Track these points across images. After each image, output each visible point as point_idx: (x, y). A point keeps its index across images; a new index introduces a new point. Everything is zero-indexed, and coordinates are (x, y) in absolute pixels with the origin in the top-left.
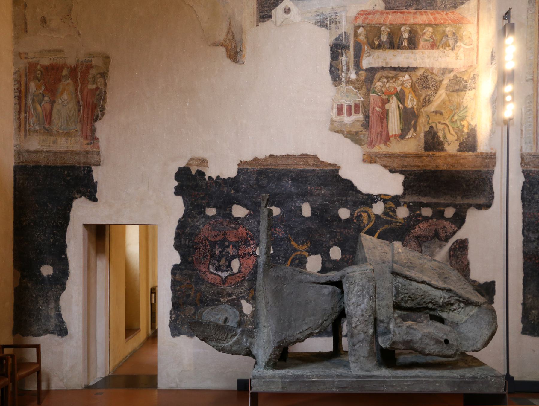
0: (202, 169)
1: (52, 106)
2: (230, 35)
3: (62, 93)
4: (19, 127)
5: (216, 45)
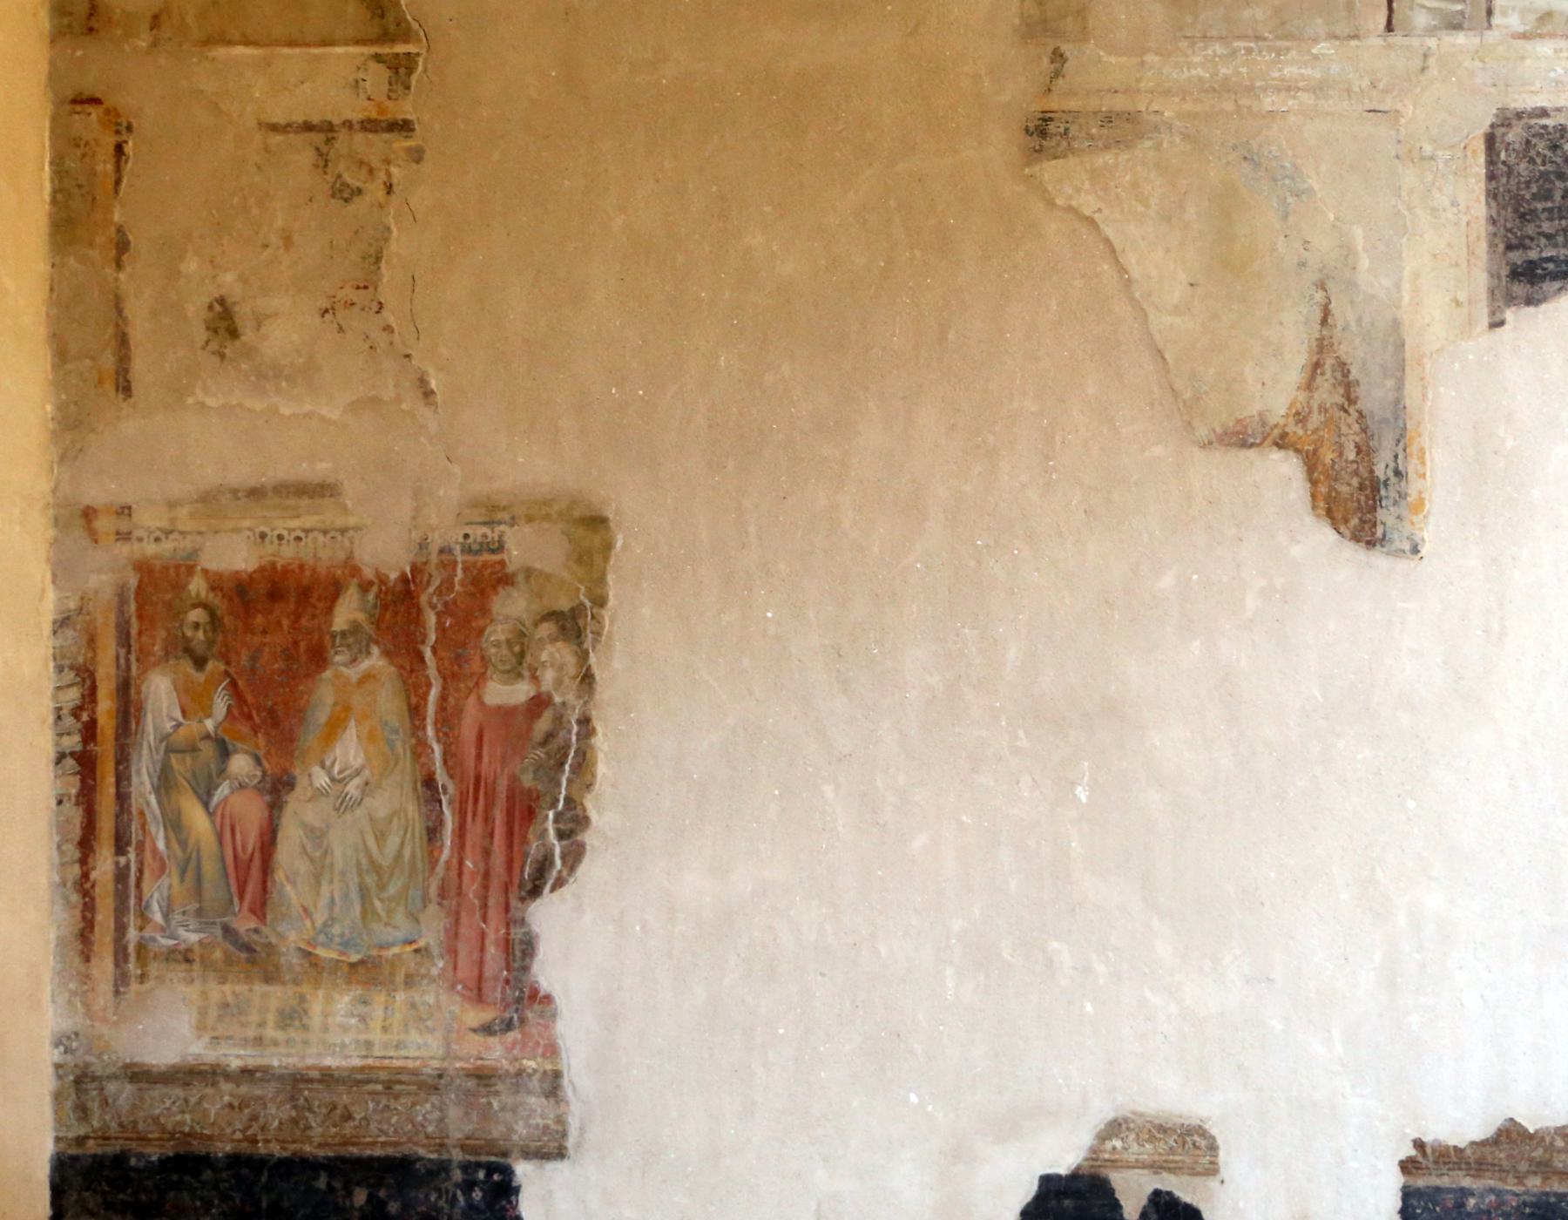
0: (1185, 1190)
1: (275, 807)
2: (1325, 382)
3: (334, 728)
4: (85, 934)
5: (1244, 445)
